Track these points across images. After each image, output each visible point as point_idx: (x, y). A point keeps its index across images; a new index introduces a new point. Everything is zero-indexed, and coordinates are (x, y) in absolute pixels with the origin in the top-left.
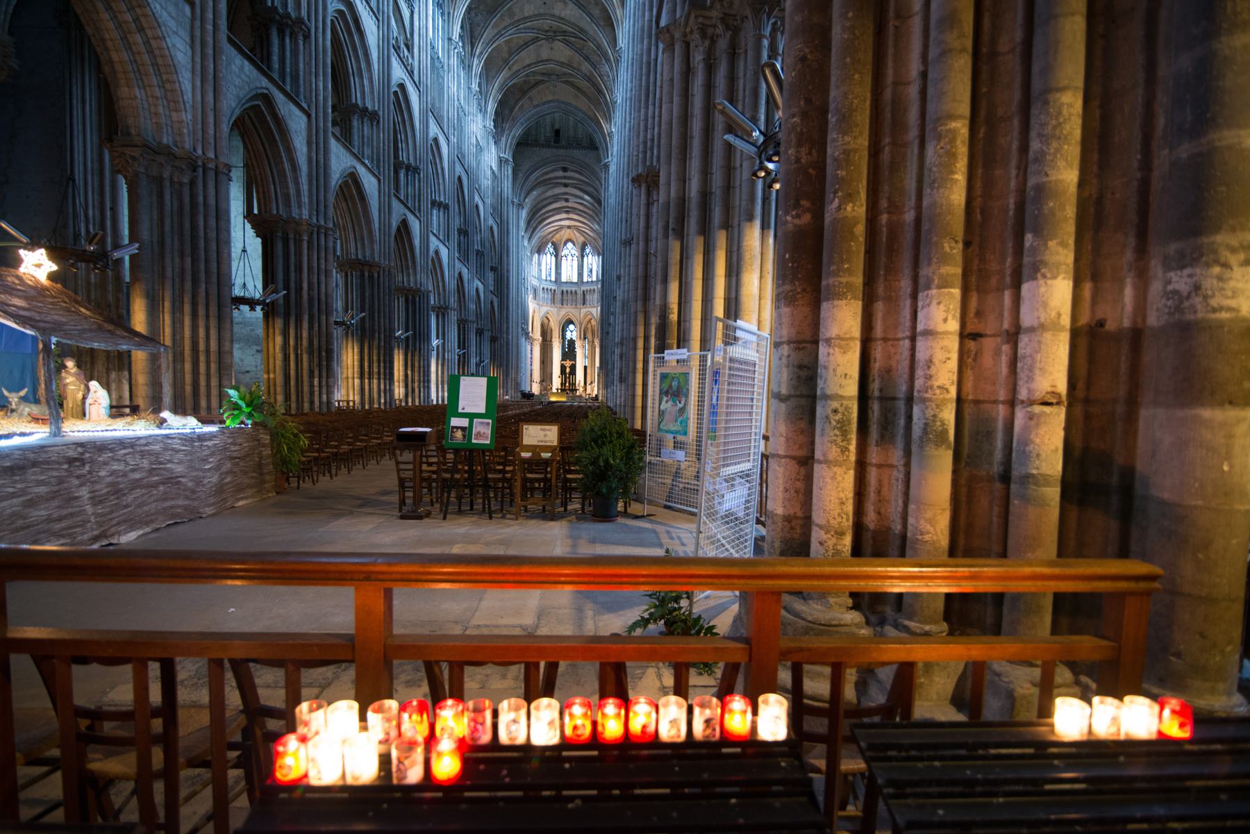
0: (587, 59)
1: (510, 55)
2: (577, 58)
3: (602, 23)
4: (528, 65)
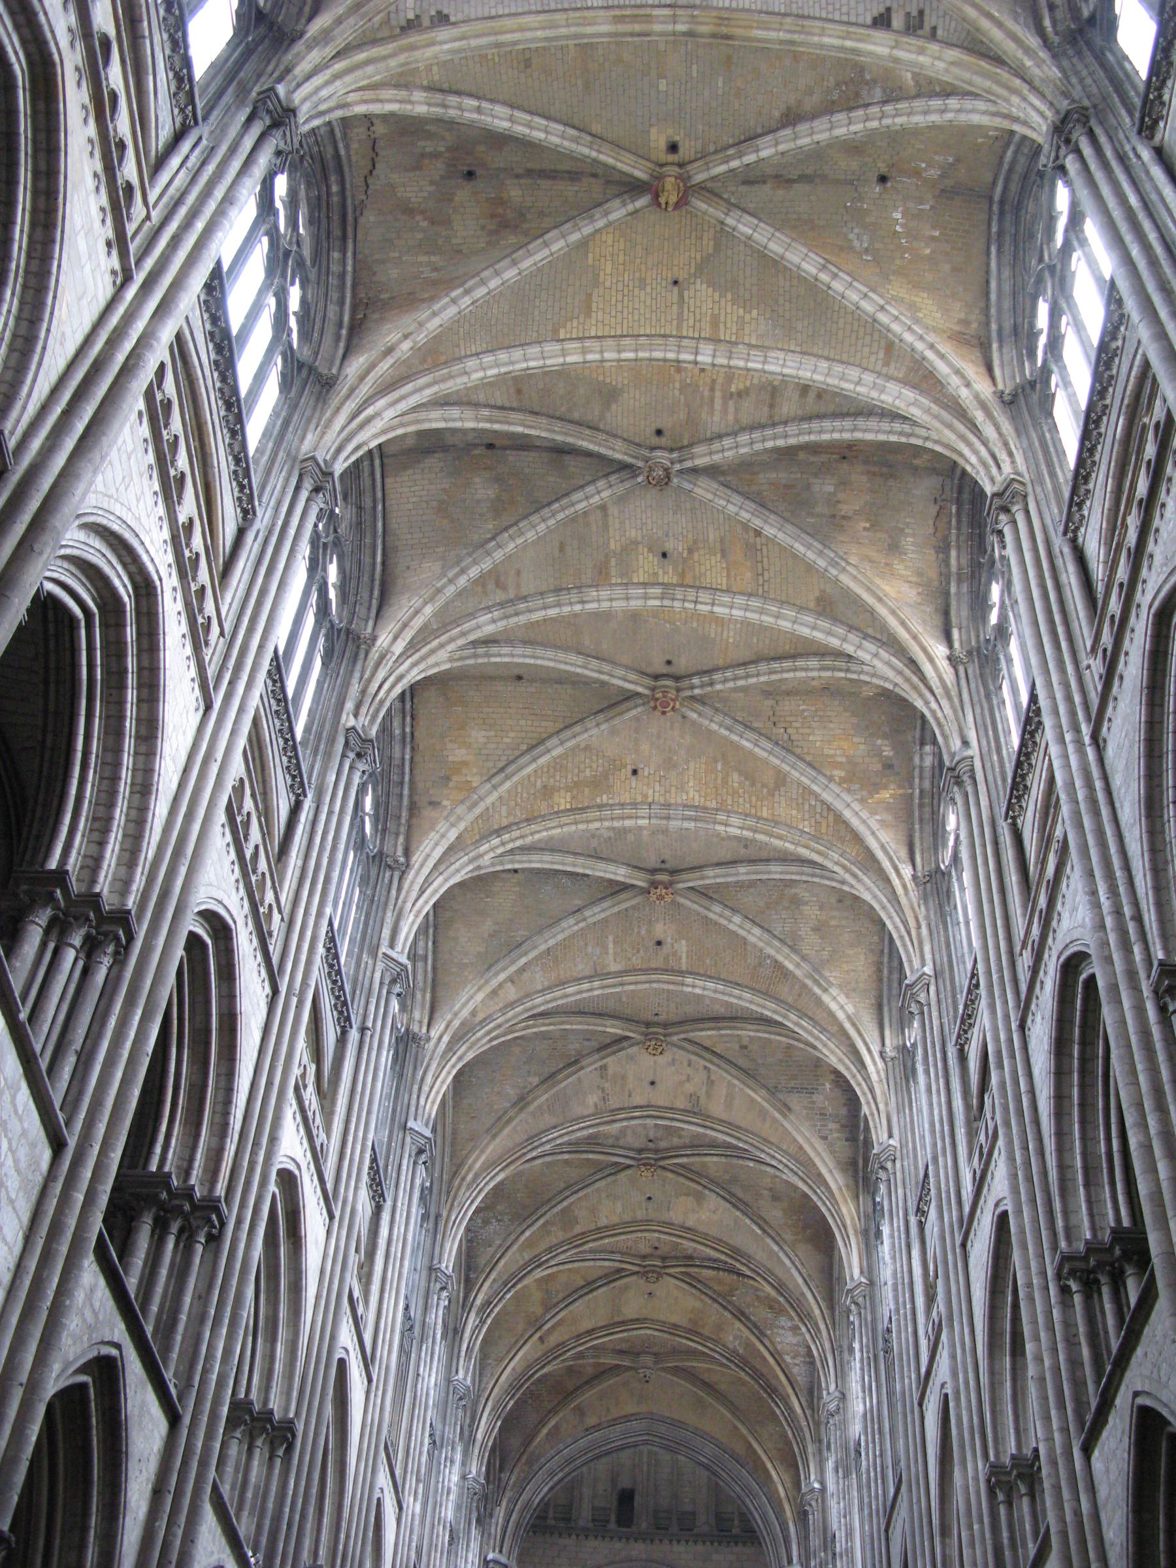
0: (741, 1315)
2: (714, 1313)
3: (788, 1236)
4: (590, 1332)
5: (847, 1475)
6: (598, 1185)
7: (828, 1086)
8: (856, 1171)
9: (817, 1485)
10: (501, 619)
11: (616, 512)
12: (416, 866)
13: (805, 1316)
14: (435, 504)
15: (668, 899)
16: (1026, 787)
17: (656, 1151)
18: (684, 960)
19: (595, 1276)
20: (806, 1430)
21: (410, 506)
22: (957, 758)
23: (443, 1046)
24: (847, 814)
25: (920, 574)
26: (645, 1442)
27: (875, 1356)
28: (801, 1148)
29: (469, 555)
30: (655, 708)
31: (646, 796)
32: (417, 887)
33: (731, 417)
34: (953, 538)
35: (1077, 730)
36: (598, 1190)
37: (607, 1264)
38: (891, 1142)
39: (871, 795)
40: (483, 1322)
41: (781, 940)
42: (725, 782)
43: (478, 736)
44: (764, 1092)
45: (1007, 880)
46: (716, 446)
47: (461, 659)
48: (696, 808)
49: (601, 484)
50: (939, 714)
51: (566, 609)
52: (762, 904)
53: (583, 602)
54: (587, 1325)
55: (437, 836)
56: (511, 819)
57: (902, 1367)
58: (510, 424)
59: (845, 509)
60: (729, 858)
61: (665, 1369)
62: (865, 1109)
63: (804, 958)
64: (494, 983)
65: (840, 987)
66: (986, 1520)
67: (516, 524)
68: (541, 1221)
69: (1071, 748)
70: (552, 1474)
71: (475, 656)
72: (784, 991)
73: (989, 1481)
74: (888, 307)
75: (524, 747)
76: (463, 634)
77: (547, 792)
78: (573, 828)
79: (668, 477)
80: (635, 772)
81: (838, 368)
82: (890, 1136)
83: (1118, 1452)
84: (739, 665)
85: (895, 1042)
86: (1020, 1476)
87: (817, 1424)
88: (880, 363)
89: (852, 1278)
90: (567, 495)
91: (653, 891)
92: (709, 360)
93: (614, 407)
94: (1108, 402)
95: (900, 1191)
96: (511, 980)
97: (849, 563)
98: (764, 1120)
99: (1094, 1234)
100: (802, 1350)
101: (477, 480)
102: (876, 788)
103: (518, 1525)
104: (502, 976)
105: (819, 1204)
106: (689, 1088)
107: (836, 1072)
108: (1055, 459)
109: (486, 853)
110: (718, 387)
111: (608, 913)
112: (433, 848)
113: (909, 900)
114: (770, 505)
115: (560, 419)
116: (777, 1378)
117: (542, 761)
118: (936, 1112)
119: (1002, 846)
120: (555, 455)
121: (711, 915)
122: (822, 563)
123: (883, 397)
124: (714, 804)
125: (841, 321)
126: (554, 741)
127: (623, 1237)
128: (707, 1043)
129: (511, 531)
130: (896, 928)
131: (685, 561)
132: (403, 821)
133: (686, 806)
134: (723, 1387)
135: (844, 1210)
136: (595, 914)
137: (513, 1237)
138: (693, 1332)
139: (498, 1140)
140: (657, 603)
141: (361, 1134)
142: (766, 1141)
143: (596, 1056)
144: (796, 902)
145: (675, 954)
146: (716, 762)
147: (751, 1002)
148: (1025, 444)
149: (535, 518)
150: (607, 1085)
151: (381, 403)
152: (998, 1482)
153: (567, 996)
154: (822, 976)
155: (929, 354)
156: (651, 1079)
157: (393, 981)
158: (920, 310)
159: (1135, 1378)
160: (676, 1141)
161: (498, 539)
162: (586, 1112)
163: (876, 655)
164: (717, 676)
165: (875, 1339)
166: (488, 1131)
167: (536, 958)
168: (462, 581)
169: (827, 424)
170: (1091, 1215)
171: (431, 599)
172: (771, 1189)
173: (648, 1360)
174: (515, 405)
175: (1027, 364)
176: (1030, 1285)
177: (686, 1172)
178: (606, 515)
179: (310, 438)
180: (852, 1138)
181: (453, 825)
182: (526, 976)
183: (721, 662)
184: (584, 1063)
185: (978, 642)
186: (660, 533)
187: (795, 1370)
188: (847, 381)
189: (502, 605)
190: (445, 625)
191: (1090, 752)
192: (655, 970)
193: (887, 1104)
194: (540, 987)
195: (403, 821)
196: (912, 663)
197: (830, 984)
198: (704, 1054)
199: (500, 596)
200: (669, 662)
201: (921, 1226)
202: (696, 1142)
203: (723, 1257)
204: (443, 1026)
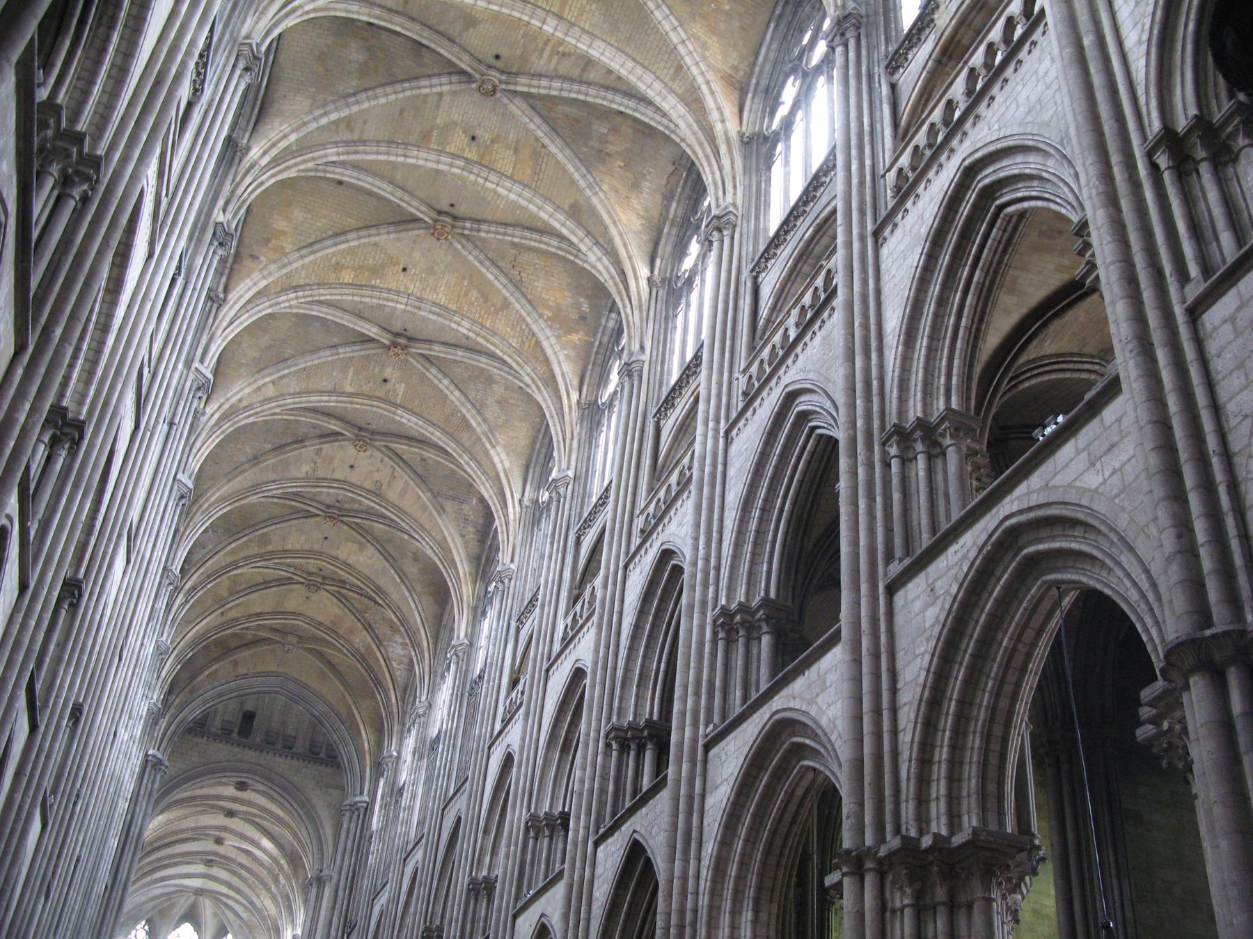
0: (369, 628)
1: (231, 594)
2: (350, 621)
3: (418, 588)
4: (257, 615)
5: (420, 758)
6: (292, 522)
7: (475, 501)
8: (479, 565)
9: (395, 754)
11: (448, 100)
12: (231, 303)
13: (416, 644)
14: (317, 53)
16: (673, 404)
17: (340, 509)
18: (400, 397)
21: (298, 49)
22: (633, 359)
23: (213, 421)
24: (545, 344)
25: (646, 210)
28: (445, 538)
29: (334, 102)
30: (433, 234)
32: (228, 319)
33: (552, 66)
35: (717, 421)
37: (283, 573)
38: (512, 566)
39: (566, 334)
40: (187, 602)
42: (466, 294)
43: (298, 215)
44: (429, 494)
45: (643, 460)
46: (535, 82)
48: (441, 306)
49: (445, 79)
50: (630, 318)
52: (466, 376)
53: (405, 156)
55: (251, 283)
56: (307, 281)
57: (483, 720)
58: (392, 23)
59: (611, 148)
60: (453, 341)
61: (303, 648)
62: (497, 522)
63: (485, 420)
64: (261, 382)
65: (504, 447)
67: (373, 88)
68: (245, 539)
69: (710, 434)
72: (465, 437)
73: (527, 823)
74: (687, 42)
75: (330, 233)
76: (314, 159)
77: (338, 267)
78: (350, 298)
79: (495, 90)
80: (404, 270)
81: (639, 71)
82: (512, 561)
83: (615, 855)
84: (501, 224)
87: (405, 713)
88: (669, 77)
89: (458, 637)
90: (417, 78)
91: (392, 348)
92: (551, 30)
93: (471, 30)
94: (808, 209)
95: (509, 601)
96: (273, 382)
98: (424, 512)
99: (635, 718)
100: (406, 660)
101: (353, 45)
102: (570, 331)
103: (174, 733)
104: (268, 379)
105: (448, 580)
106: (377, 476)
107: (482, 499)
108: (762, 208)
109: (283, 302)
111: (356, 354)
112: (246, 292)
114: (559, 130)
115: (429, 27)
116: (384, 675)
118: (551, 575)
119: (646, 434)
121: (428, 374)
122: (582, 184)
124: (454, 307)
125: (653, 36)
127: (301, 560)
129: (370, 93)
131: (487, 147)
132: (228, 265)
133: (434, 304)
134: (341, 668)
135: (464, 590)
136: (345, 352)
137: (222, 546)
138: (332, 630)
139: (231, 484)
140: (457, 171)
141: (157, 503)
142: (422, 526)
143: (318, 441)
145: (395, 391)
146: (464, 279)
148: (747, 183)
149: (389, 89)
150: (319, 461)
152: (532, 826)
153: (310, 402)
155: (704, 88)
156: (351, 463)
157: (199, 389)
159: (637, 824)
160: (356, 506)
161: (359, 96)
163: (599, 259)
164: (484, 227)
165: (465, 684)
168: (324, 121)
169: (618, 98)
170: (636, 705)
171: (297, 129)
172: (414, 553)
173: (294, 640)
174: (400, 9)
175: (766, 119)
176: (588, 735)
177: (358, 528)
178: (440, 99)
179: (249, 22)
180: (482, 541)
181: (264, 277)
182: (285, 381)
183: (489, 218)
184: (307, 443)
186: (475, 123)
187: (398, 673)
188: (641, 81)
189: (347, 143)
190: (301, 149)
191: (721, 441)
192: (378, 399)
193: (515, 538)
194: (292, 391)
195: (228, 265)
196: (622, 274)
199: (347, 136)
200: (452, 205)
201: (518, 631)
203: (368, 590)
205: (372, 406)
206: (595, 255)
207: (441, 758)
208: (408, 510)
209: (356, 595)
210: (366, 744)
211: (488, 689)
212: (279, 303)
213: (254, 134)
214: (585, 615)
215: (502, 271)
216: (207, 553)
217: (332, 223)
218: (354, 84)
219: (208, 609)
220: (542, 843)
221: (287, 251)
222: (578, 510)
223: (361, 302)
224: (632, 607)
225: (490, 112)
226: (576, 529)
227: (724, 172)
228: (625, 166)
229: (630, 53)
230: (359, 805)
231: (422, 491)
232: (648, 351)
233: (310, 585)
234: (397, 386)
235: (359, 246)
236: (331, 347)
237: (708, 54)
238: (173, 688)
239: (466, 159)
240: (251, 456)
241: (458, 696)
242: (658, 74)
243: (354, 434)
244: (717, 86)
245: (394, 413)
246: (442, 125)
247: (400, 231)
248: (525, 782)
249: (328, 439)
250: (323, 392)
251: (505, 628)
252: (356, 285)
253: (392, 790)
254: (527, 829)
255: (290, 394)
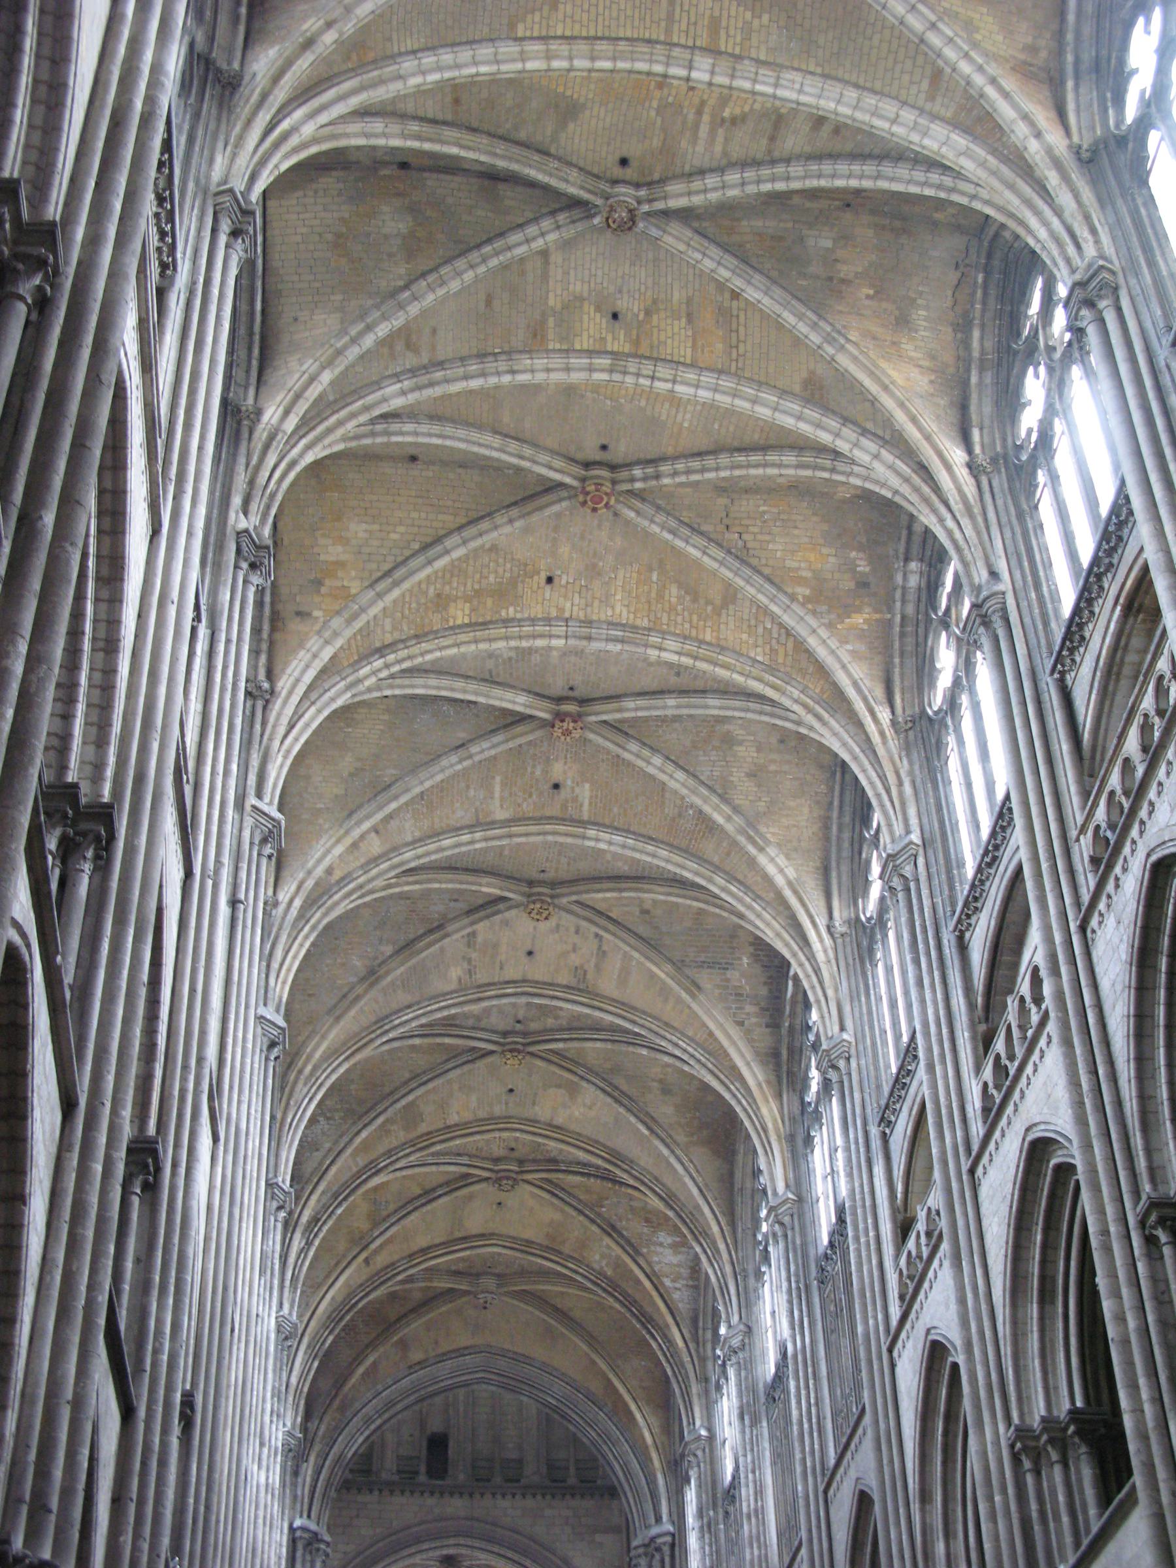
0: (611, 1230)
1: (375, 1225)
2: (577, 1227)
3: (681, 1138)
4: (424, 1251)
5: (755, 1422)
6: (452, 1075)
7: (745, 960)
8: (778, 1065)
9: (703, 1433)
10: (412, 390)
11: (560, 261)
12: (284, 693)
13: (701, 1233)
14: (329, 237)
15: (576, 734)
16: (1083, 638)
17: (525, 1034)
18: (586, 807)
19: (434, 1184)
20: (689, 1367)
21: (299, 238)
22: (984, 593)
23: (294, 912)
24: (812, 642)
25: (933, 358)
26: (480, 1381)
27: (807, 1287)
28: (711, 1034)
29: (377, 307)
30: (584, 503)
31: (562, 610)
32: (285, 721)
33: (718, 148)
34: (978, 314)
36: (449, 1082)
37: (452, 1168)
38: (845, 1036)
40: (309, 1244)
41: (710, 788)
42: (660, 597)
43: (357, 529)
44: (669, 967)
45: (1055, 747)
46: (697, 185)
47: (357, 437)
49: (546, 224)
50: (958, 535)
51: (493, 380)
52: (688, 743)
53: (513, 372)
54: (422, 1242)
55: (309, 656)
57: (864, 1305)
58: (443, 142)
59: (845, 270)
60: (655, 686)
61: (508, 1294)
63: (736, 810)
64: (356, 833)
65: (779, 845)
66: (1011, 1490)
67: (435, 269)
70: (368, 1421)
71: (373, 434)
72: (709, 848)
73: (1012, 1446)
74: (940, 25)
75: (416, 546)
76: (367, 408)
77: (441, 602)
78: (473, 647)
79: (633, 220)
80: (550, 580)
81: (871, 100)
82: (842, 1029)
85: (845, 915)
86: (1051, 1441)
87: (703, 1360)
88: (922, 96)
89: (775, 1193)
90: (502, 234)
91: (558, 724)
92: (706, 77)
93: (571, 126)
95: (857, 1095)
96: (375, 830)
97: (848, 340)
98: (666, 1000)
101: (385, 209)
102: (848, 610)
104: (367, 825)
105: (733, 1103)
106: (575, 960)
109: (366, 677)
110: (707, 110)
112: (304, 671)
113: (888, 751)
114: (754, 261)
115: (503, 138)
116: (654, 1304)
117: (440, 564)
118: (930, 1011)
119: (1047, 705)
120: (486, 182)
121: (626, 755)
122: (815, 338)
123: (927, 142)
125: (877, 38)
126: (455, 539)
127: (477, 1137)
128: (601, 906)
130: (871, 783)
133: (611, 624)
134: (577, 1314)
135: (764, 1111)
136: (482, 750)
137: (346, 1139)
138: (551, 1249)
139: (342, 1023)
140: (605, 376)
141: (240, 1035)
143: (466, 921)
144: (729, 741)
145: (575, 799)
147: (667, 861)
148: (1112, 219)
149: (461, 264)
150: (474, 955)
151: (298, 114)
152: (1025, 1448)
153: (442, 850)
154: (757, 831)
155: (990, 91)
156: (528, 947)
157: (264, 841)
158: (977, 29)
160: (550, 1022)
161: (414, 287)
162: (448, 988)
163: (876, 457)
164: (665, 468)
165: (806, 1266)
166: (329, 1012)
167: (406, 804)
168: (369, 341)
169: (842, 167)
171: (329, 364)
172: (661, 1081)
173: (489, 1283)
174: (449, 117)
175: (1111, 112)
177: (561, 1060)
178: (547, 262)
179: (220, 162)
180: (774, 1025)
181: (327, 642)
182: (394, 824)
183: (670, 451)
184: (450, 928)
185: (1004, 446)
186: (612, 289)
187: (676, 1296)
188: (881, 117)
189: (413, 372)
190: (344, 397)
192: (550, 819)
193: (836, 990)
194: (409, 838)
196: (923, 469)
197: (768, 842)
198: (596, 919)
199: (411, 361)
200: (604, 447)
201: (885, 1139)
202: (575, 1024)
203: (600, 1162)
204: (293, 887)
205: (545, 833)
206: (867, 451)
207: (799, 1402)
208: (639, 1004)
209: (578, 1178)
210: (647, 1435)
211: (858, 1250)
212: (360, 681)
213: (262, 389)
214: (1019, 1052)
215: (710, 540)
216: (325, 1157)
217: (416, 530)
218: (402, 271)
219: (344, 1256)
220: (1051, 1479)
221: (353, 591)
222: (946, 892)
223: (491, 655)
224: (1119, 987)
225: (633, 264)
226: (952, 924)
227: (1067, 215)
228: (877, 292)
229: (847, 77)
230: (659, 1541)
231: (656, 964)
232: (1005, 575)
233: (500, 1179)
234: (577, 790)
235: (467, 556)
236: (458, 747)
237: (978, 37)
238: (312, 1407)
239: (612, 353)
240: (363, 972)
241: (799, 1293)
242: (903, 97)
243: (523, 894)
244: (1008, 84)
245: (584, 837)
246: (559, 306)
247: (529, 514)
248: (988, 1374)
249: (482, 914)
250: (461, 828)
251: (861, 1140)
252: (476, 624)
253: (714, 1495)
254: (1016, 1459)
255: (407, 844)
